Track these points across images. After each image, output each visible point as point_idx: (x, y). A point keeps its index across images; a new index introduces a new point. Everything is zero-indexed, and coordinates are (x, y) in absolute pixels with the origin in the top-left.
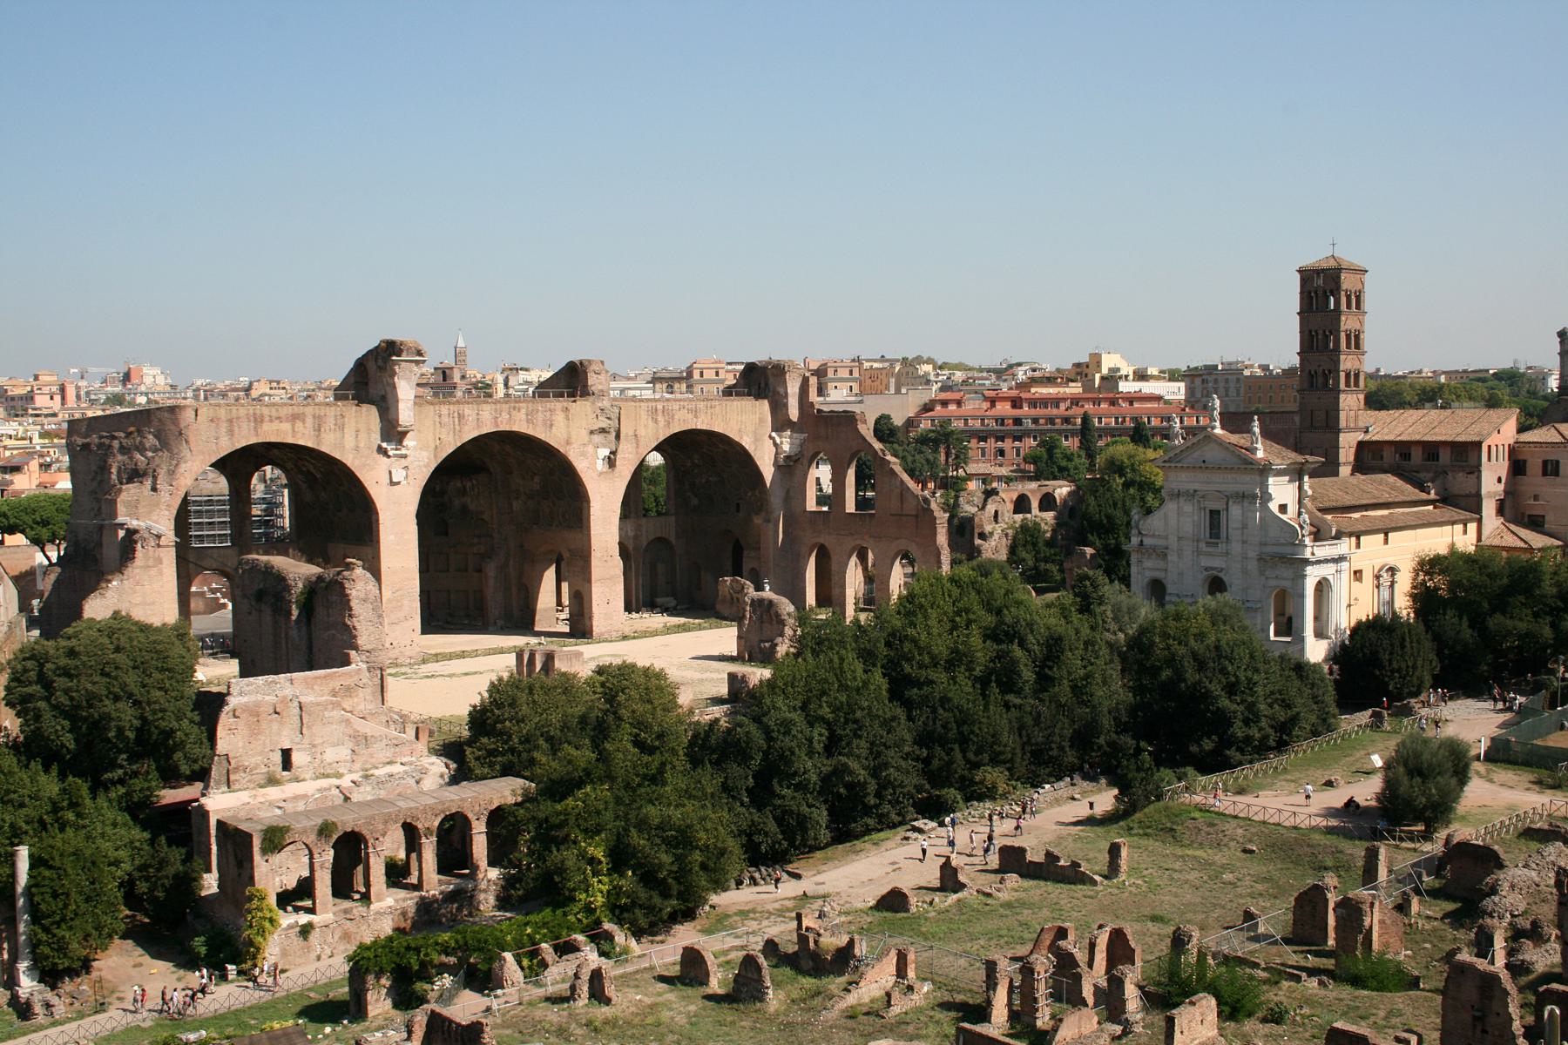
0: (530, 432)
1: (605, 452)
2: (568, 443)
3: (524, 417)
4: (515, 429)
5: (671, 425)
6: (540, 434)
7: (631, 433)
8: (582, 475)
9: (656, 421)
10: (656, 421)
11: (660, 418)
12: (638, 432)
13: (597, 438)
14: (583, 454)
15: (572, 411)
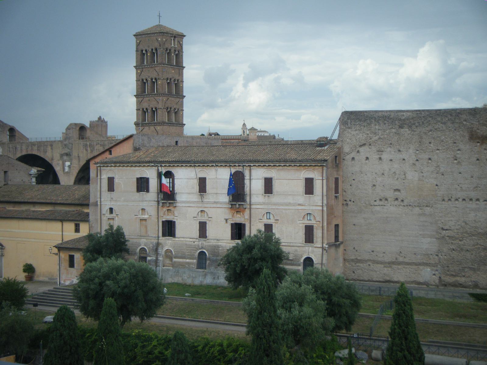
0: (38, 154)
1: (68, 164)
2: (52, 159)
3: (36, 148)
4: (33, 153)
5: (93, 152)
6: (42, 155)
7: (77, 155)
8: (57, 173)
9: (87, 150)
10: (87, 150)
11: (89, 149)
12: (80, 155)
13: (65, 158)
14: (58, 164)
15: (54, 146)
